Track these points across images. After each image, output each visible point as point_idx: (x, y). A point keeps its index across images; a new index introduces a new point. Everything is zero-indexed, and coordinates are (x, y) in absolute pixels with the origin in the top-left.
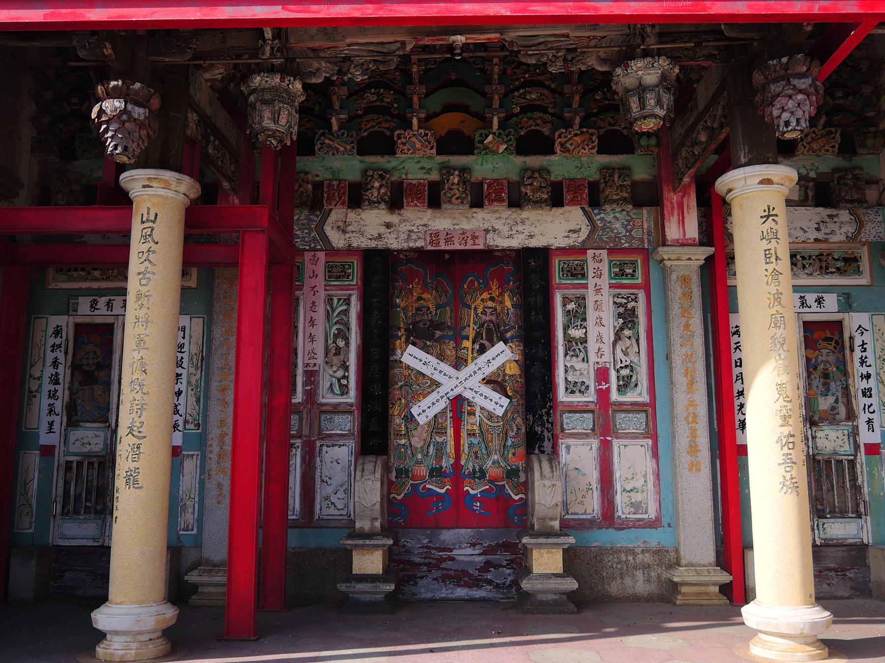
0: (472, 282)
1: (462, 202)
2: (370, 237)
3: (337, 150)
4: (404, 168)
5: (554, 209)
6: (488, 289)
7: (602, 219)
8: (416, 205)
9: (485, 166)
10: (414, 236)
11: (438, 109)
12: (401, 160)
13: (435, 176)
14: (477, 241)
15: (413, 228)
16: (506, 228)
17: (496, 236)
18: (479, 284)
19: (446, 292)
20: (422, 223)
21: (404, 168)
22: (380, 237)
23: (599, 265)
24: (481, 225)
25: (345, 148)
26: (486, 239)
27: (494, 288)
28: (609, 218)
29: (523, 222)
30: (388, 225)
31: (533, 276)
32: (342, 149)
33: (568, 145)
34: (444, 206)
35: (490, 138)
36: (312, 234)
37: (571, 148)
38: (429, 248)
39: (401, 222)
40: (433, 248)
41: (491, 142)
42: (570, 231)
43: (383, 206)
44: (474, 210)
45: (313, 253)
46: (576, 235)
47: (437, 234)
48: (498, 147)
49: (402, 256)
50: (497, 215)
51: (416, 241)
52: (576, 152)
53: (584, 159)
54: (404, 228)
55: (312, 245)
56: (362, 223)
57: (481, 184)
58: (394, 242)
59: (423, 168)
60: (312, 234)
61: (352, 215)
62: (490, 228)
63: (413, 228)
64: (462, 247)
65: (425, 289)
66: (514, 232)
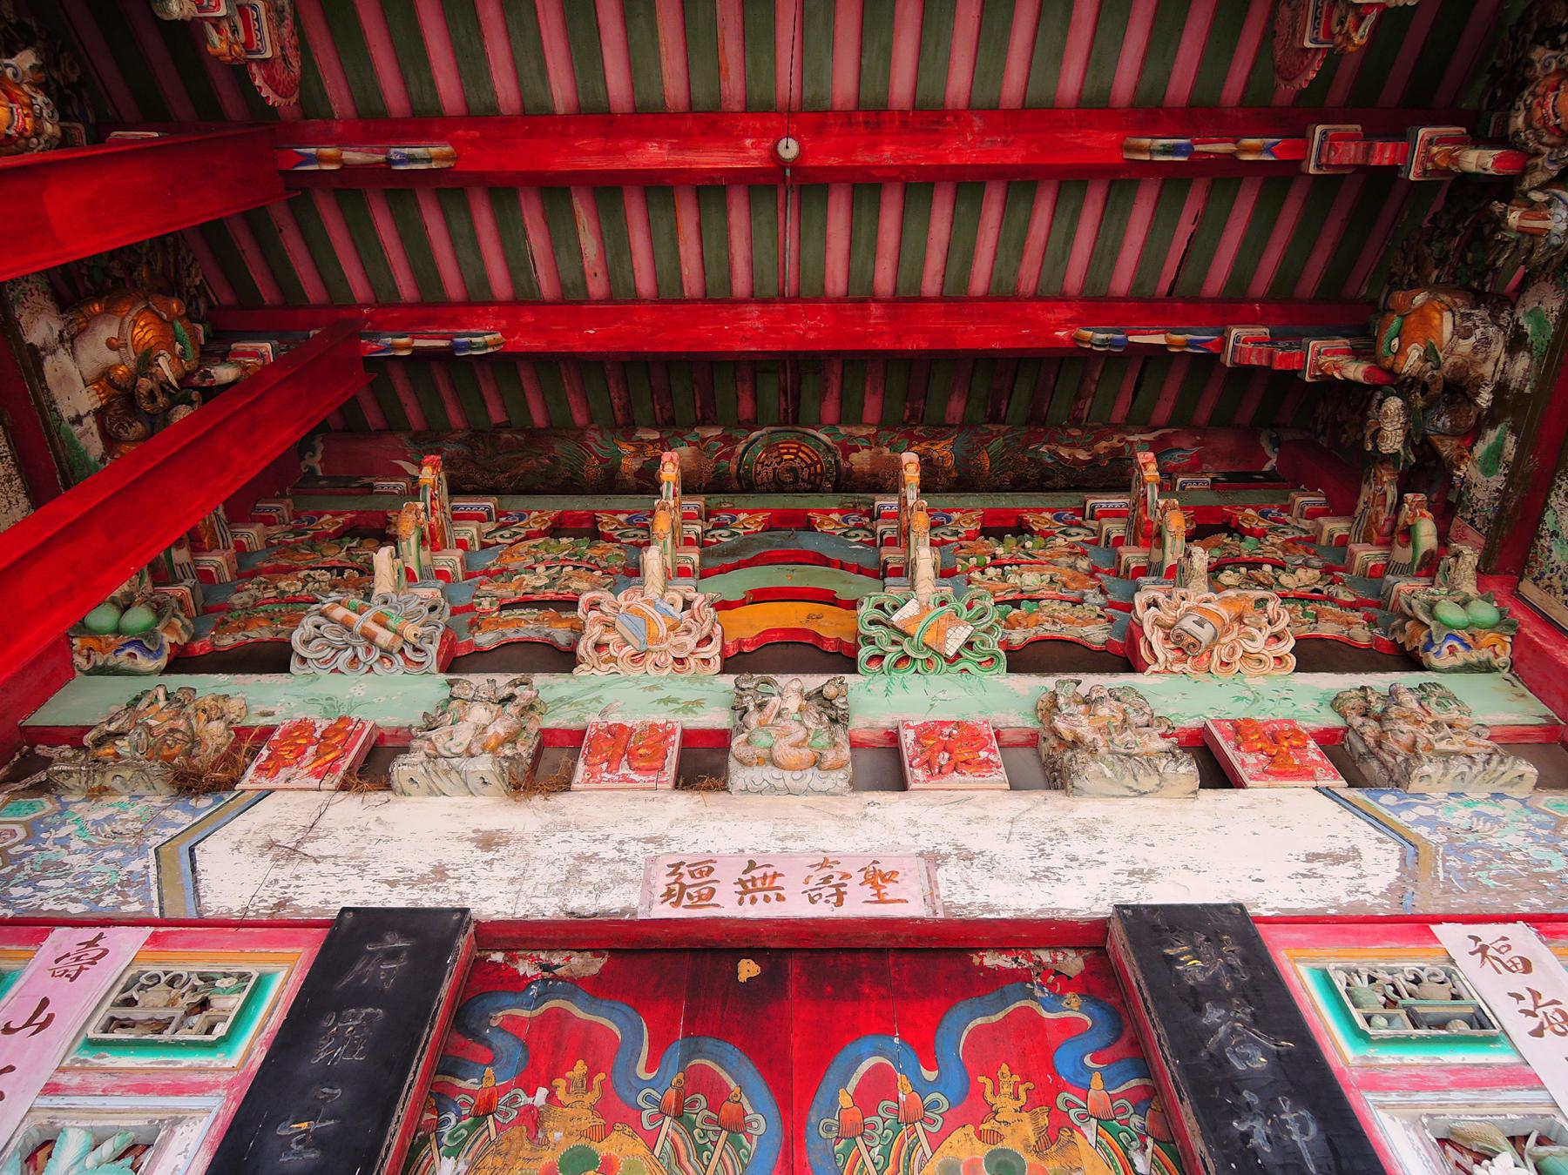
0: (877, 1088)
1: (817, 763)
2: (392, 874)
3: (370, 638)
4: (598, 700)
5: (1209, 795)
6: (972, 1110)
7: (1430, 822)
8: (625, 779)
9: (898, 696)
10: (595, 874)
11: (740, 597)
12: (594, 682)
13: (714, 717)
14: (891, 890)
15: (595, 848)
16: (1018, 849)
17: (977, 876)
18: (921, 1088)
19: (736, 1127)
20: (643, 832)
21: (598, 700)
22: (440, 872)
23: (1533, 980)
24: (906, 841)
25: (398, 633)
26: (932, 883)
27: (1006, 1105)
28: (1459, 816)
29: (1088, 830)
30: (488, 842)
31: (1213, 1015)
32: (384, 637)
33: (1188, 624)
34: (739, 776)
35: (911, 609)
36: (136, 865)
37: (1205, 634)
38: (663, 911)
39: (547, 830)
40: (680, 913)
41: (914, 619)
42: (1312, 857)
43: (484, 764)
44: (868, 796)
45: (90, 933)
46: (1345, 870)
47: (705, 868)
48: (941, 632)
49: (525, 968)
50: (969, 811)
51: (600, 889)
52: (1221, 652)
53: (1258, 683)
54: (559, 848)
55: (109, 900)
56: (378, 831)
57: (893, 738)
58: (493, 897)
59: (667, 701)
60: (136, 865)
61: (350, 809)
62: (944, 849)
63: (595, 848)
64: (823, 910)
65: (615, 1112)
66: (1057, 861)
